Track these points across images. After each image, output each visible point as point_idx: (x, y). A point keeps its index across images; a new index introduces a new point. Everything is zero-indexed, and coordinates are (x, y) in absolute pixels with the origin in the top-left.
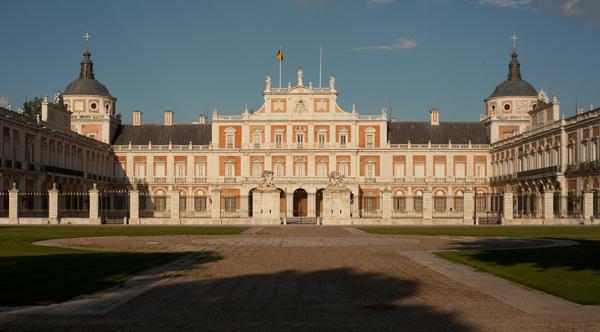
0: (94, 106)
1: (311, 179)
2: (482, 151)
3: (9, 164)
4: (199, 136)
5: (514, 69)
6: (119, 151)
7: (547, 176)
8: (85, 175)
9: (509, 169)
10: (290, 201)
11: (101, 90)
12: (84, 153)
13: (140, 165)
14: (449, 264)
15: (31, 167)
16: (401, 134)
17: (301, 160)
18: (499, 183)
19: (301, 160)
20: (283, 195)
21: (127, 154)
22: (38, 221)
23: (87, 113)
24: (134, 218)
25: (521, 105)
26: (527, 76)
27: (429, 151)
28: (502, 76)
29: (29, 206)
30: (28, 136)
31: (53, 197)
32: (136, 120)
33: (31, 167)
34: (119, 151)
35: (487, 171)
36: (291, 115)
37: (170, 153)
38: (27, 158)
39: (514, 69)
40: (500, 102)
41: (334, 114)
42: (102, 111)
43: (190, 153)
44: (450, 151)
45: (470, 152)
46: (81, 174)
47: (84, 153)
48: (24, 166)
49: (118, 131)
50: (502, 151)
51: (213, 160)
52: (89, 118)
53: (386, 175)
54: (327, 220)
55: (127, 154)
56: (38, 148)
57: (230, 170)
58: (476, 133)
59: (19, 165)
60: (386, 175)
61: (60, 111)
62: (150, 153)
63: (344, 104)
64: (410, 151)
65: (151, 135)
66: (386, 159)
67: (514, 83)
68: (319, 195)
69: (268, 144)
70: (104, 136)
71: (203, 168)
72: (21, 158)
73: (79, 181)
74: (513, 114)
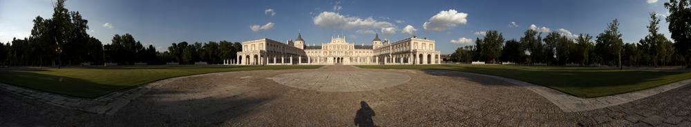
1: (340, 55)
2: (372, 51)
4: (319, 48)
5: (377, 36)
6: (305, 51)
7: (387, 55)
9: (378, 54)
10: (336, 60)
11: (302, 40)
13: (309, 53)
15: (284, 54)
16: (356, 47)
17: (338, 52)
18: (375, 57)
19: (338, 52)
20: (335, 58)
21: (306, 51)
22: (280, 64)
24: (300, 63)
25: (378, 42)
26: (379, 37)
27: (362, 51)
28: (375, 37)
29: (279, 61)
31: (275, 59)
32: (308, 45)
34: (305, 51)
35: (372, 55)
36: (337, 43)
37: (314, 51)
39: (377, 36)
40: (375, 42)
41: (345, 43)
42: (302, 44)
43: (318, 51)
44: (366, 51)
45: (369, 51)
49: (305, 47)
50: (375, 51)
51: (322, 52)
52: (298, 45)
53: (354, 55)
54: (344, 63)
55: (306, 51)
58: (371, 48)
60: (354, 55)
61: (291, 43)
62: (311, 51)
63: (347, 42)
64: (358, 50)
65: (311, 48)
66: (354, 52)
67: (377, 39)
68: (342, 58)
69: (332, 49)
70: (302, 48)
71: (321, 53)
74: (378, 44)
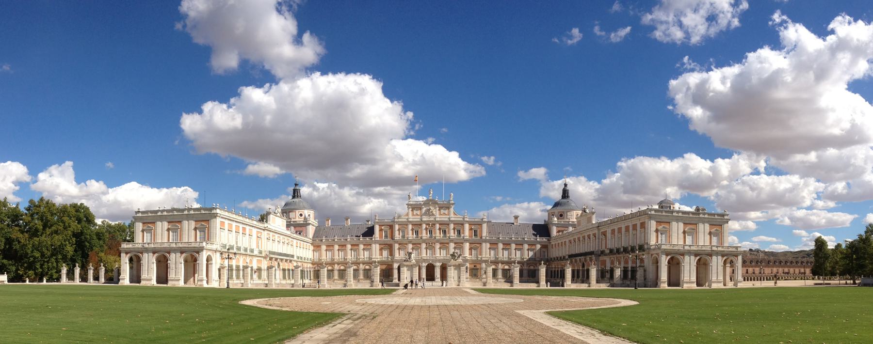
0: (301, 215)
3: (246, 250)
8: (295, 258)
12: (295, 244)
14: (557, 320)
23: (297, 219)
30: (258, 232)
33: (261, 252)
38: (258, 246)
46: (293, 256)
47: (295, 244)
48: (256, 253)
51: (376, 248)
56: (264, 240)
57: (385, 253)
59: (252, 251)
72: (254, 246)
73: (291, 261)
